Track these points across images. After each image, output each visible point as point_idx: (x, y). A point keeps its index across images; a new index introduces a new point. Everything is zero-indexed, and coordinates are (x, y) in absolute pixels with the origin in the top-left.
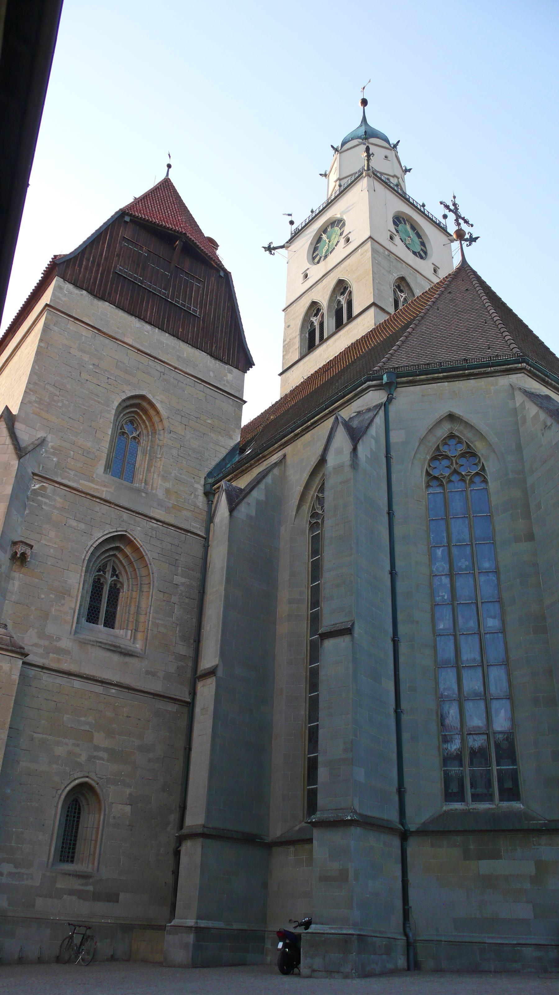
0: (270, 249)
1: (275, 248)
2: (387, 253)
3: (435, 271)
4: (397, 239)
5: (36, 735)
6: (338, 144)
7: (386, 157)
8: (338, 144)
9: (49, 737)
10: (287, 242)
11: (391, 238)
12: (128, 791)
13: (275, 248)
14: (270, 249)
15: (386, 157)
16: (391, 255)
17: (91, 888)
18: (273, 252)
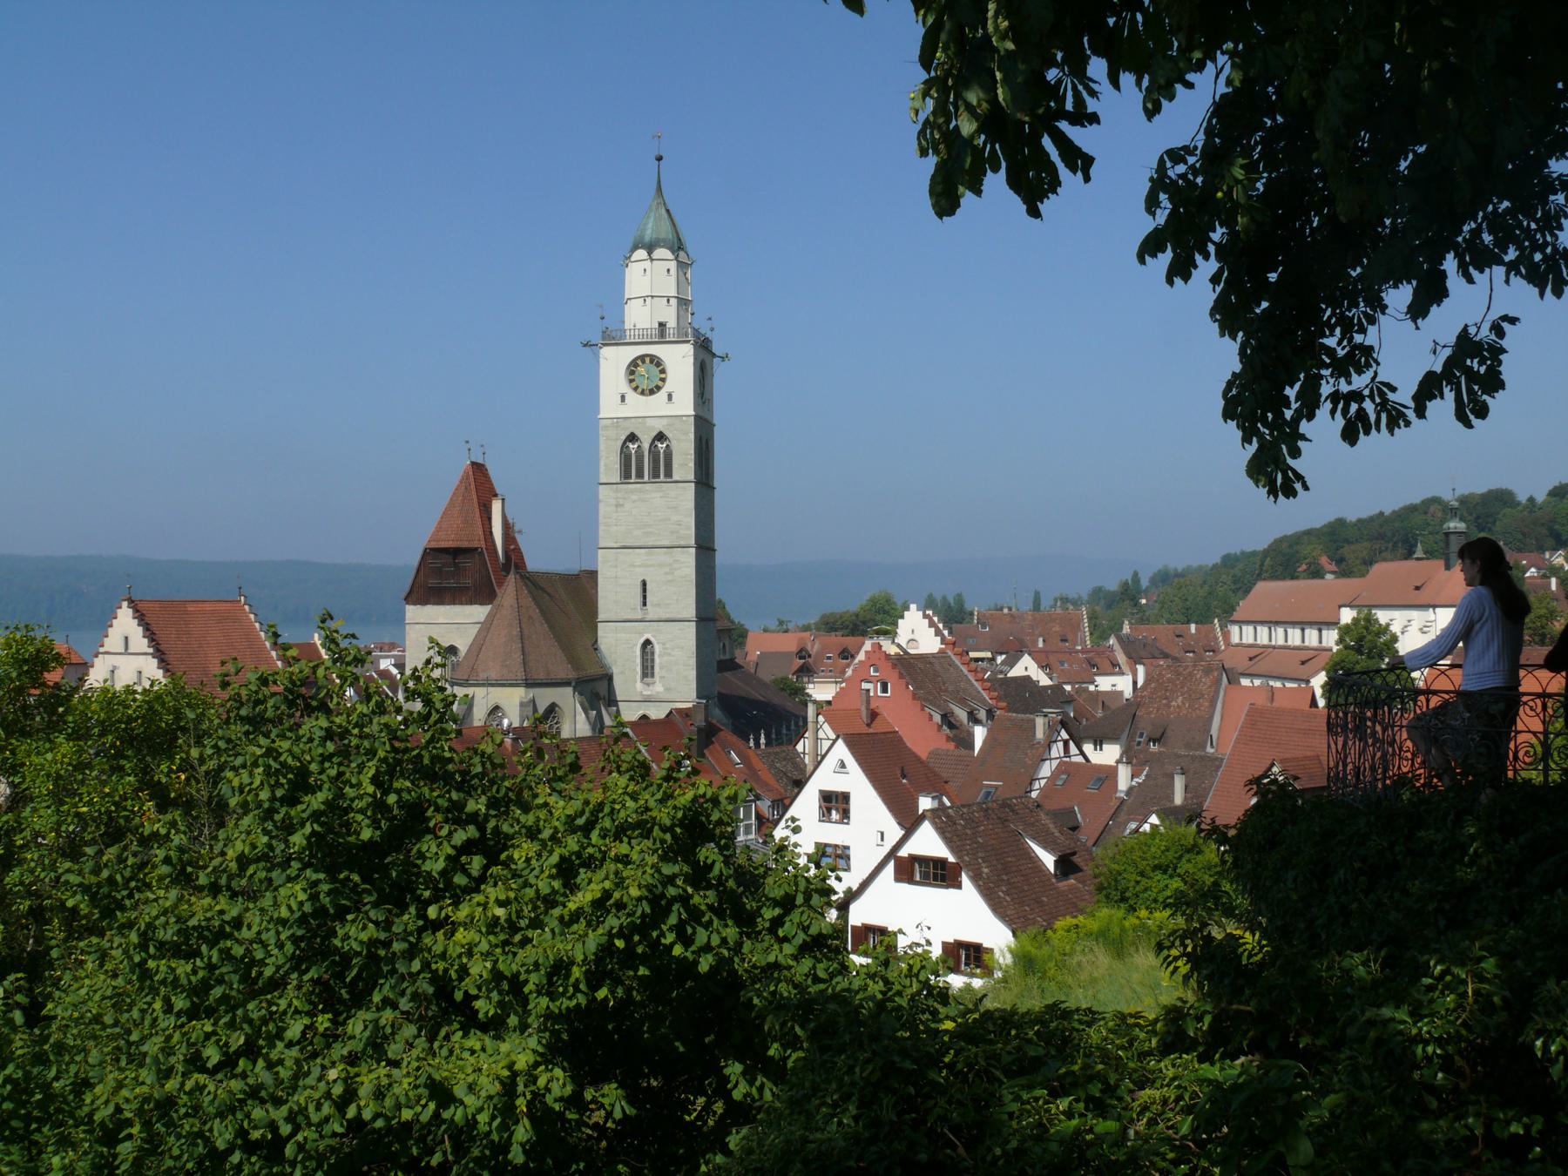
3: (670, 397)
11: (623, 398)
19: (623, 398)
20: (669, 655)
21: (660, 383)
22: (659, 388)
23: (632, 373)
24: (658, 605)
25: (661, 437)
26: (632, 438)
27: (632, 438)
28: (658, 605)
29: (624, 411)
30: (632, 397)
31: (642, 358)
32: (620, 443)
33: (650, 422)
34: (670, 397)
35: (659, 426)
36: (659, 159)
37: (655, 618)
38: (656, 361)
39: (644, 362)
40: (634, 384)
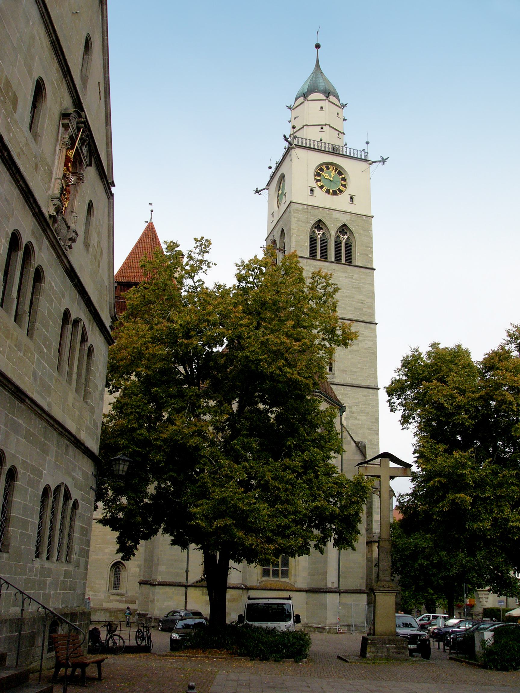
0: (258, 192)
1: (260, 191)
2: (305, 207)
3: (352, 198)
4: (317, 191)
5: (96, 545)
6: (291, 103)
7: (322, 108)
8: (291, 103)
9: (102, 546)
10: (267, 185)
11: (312, 190)
12: (137, 563)
13: (260, 191)
14: (258, 192)
15: (322, 108)
16: (309, 207)
17: (124, 599)
18: (260, 193)
19: (312, 190)
20: (356, 418)
21: (342, 188)
22: (341, 191)
23: (318, 174)
24: (345, 371)
25: (344, 229)
26: (319, 225)
27: (319, 225)
28: (345, 371)
29: (312, 201)
30: (317, 191)
31: (328, 165)
32: (309, 226)
33: (335, 214)
34: (352, 198)
35: (344, 219)
36: (318, 46)
37: (342, 382)
38: (340, 172)
39: (328, 168)
40: (320, 184)
